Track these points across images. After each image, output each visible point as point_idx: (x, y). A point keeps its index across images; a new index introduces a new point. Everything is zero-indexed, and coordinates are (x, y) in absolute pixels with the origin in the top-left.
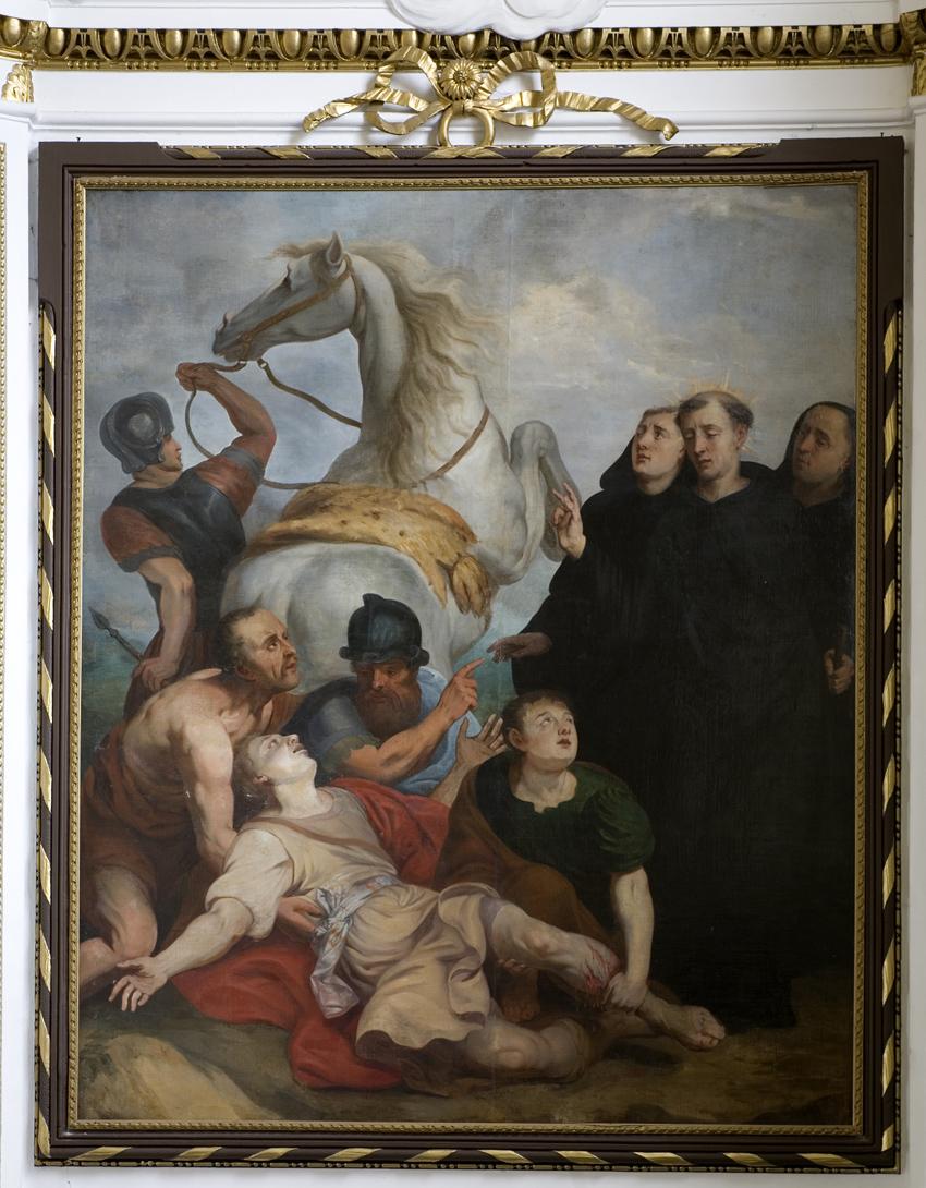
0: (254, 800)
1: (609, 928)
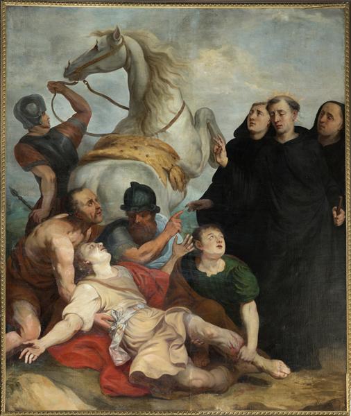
0: (83, 271)
1: (239, 325)
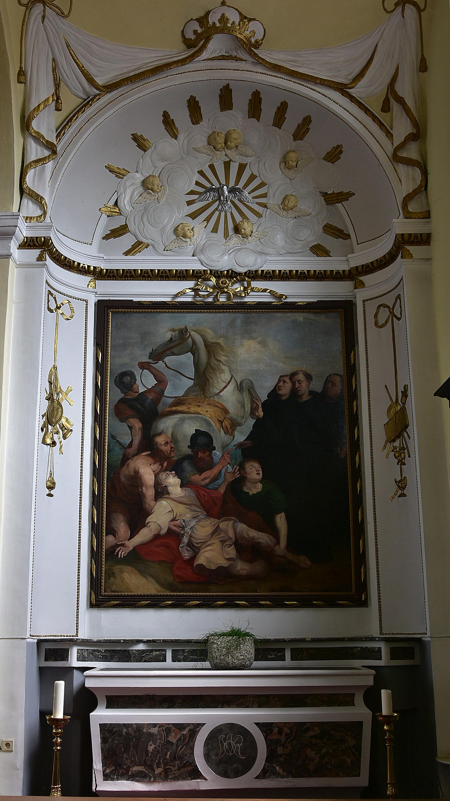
0: (161, 492)
1: (274, 531)
